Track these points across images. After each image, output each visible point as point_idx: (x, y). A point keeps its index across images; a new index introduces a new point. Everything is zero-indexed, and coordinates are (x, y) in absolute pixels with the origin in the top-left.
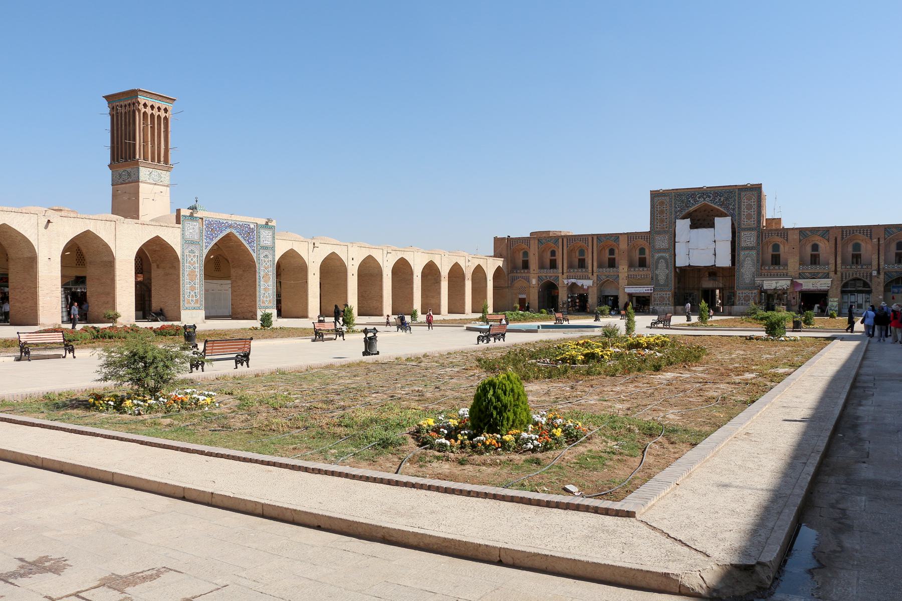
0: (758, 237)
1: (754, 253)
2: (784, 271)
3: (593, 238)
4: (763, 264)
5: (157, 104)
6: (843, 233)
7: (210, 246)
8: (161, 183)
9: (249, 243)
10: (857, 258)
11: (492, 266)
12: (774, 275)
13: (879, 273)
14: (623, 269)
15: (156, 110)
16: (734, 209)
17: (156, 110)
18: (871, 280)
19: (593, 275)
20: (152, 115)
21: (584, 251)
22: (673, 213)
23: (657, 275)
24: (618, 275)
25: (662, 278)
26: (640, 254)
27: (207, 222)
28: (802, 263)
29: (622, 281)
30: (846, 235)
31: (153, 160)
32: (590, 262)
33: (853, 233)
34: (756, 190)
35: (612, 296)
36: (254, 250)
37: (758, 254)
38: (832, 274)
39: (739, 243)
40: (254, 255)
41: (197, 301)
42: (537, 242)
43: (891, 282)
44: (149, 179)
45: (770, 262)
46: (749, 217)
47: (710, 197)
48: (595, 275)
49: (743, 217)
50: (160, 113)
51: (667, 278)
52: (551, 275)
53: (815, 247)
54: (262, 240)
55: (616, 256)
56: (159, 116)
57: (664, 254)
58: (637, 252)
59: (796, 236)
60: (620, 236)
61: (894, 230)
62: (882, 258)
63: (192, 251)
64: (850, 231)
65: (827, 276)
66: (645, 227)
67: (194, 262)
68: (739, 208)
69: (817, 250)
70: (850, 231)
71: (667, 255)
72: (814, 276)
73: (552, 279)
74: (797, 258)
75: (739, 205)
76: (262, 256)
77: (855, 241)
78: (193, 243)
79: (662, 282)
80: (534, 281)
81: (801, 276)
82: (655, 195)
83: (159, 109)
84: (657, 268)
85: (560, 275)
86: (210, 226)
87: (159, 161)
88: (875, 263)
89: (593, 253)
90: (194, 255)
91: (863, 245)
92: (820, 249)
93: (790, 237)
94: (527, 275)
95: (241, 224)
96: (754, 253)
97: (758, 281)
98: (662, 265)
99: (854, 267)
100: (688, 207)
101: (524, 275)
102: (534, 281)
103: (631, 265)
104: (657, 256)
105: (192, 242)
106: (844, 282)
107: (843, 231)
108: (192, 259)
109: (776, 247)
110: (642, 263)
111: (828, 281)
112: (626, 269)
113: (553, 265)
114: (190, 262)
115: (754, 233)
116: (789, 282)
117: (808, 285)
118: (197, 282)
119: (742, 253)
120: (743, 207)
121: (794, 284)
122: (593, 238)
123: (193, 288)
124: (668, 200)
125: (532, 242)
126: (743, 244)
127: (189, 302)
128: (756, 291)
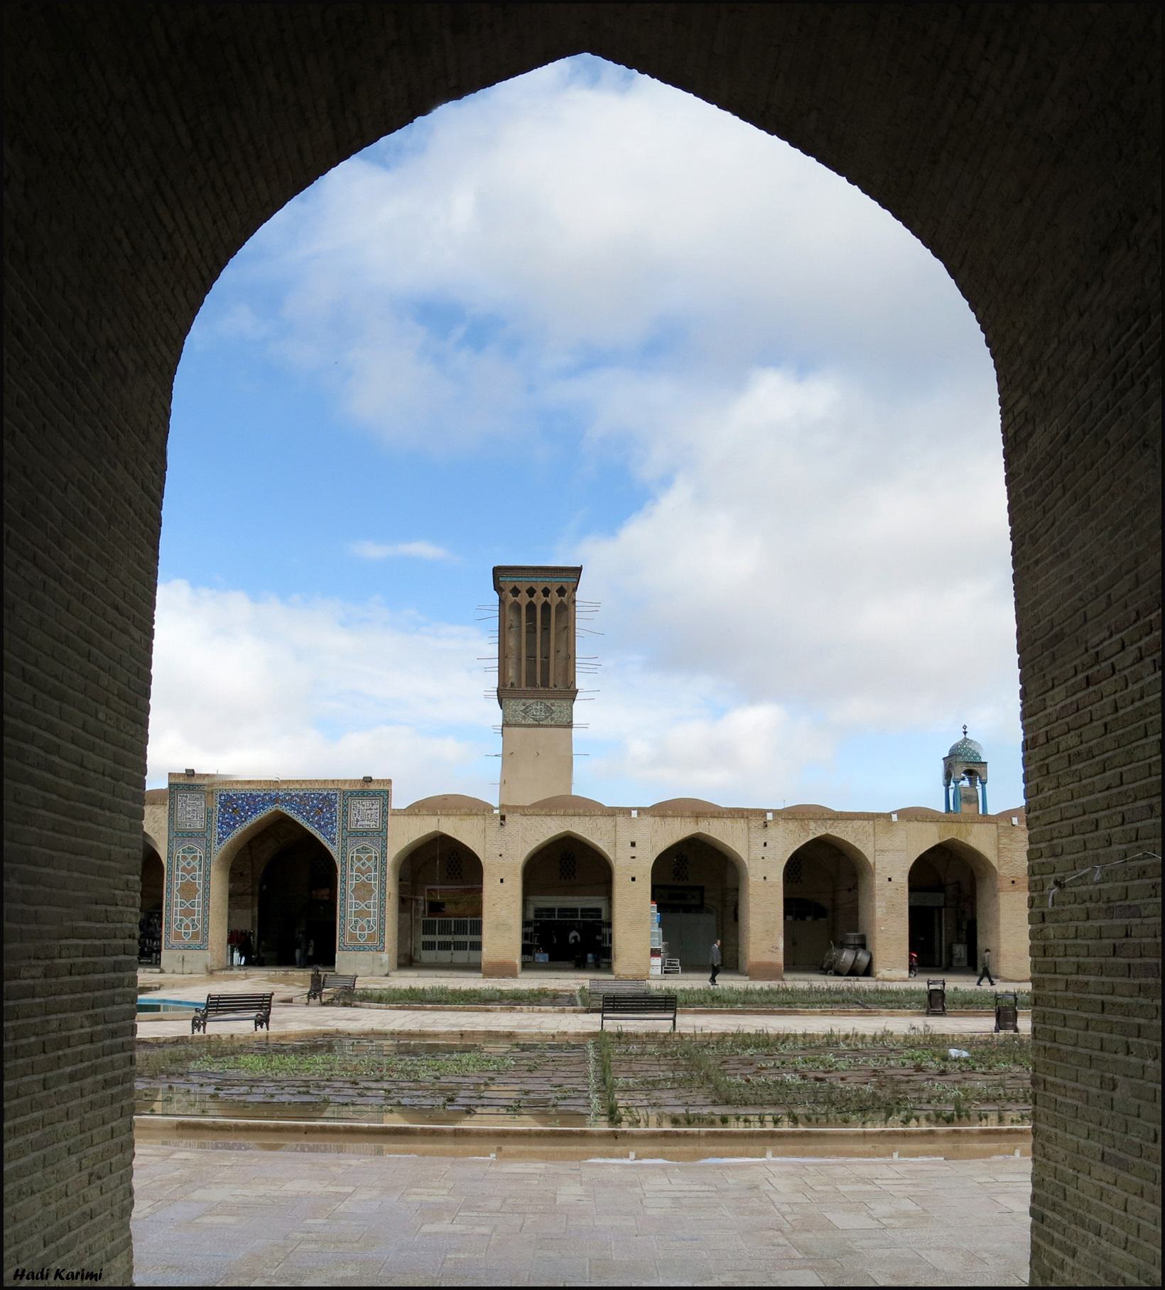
5: (540, 583)
7: (229, 840)
8: (553, 723)
9: (320, 827)
15: (539, 593)
17: (539, 593)
20: (531, 607)
27: (223, 798)
31: (531, 681)
36: (332, 840)
40: (334, 851)
41: (195, 935)
44: (524, 718)
50: (548, 599)
54: (353, 819)
56: (546, 606)
63: (191, 850)
67: (193, 867)
76: (352, 852)
78: (190, 835)
83: (546, 592)
86: (229, 804)
87: (545, 683)
90: (195, 857)
95: (301, 793)
105: (190, 835)
108: (188, 864)
114: (184, 869)
118: (176, 907)
123: (188, 913)
127: (178, 936)
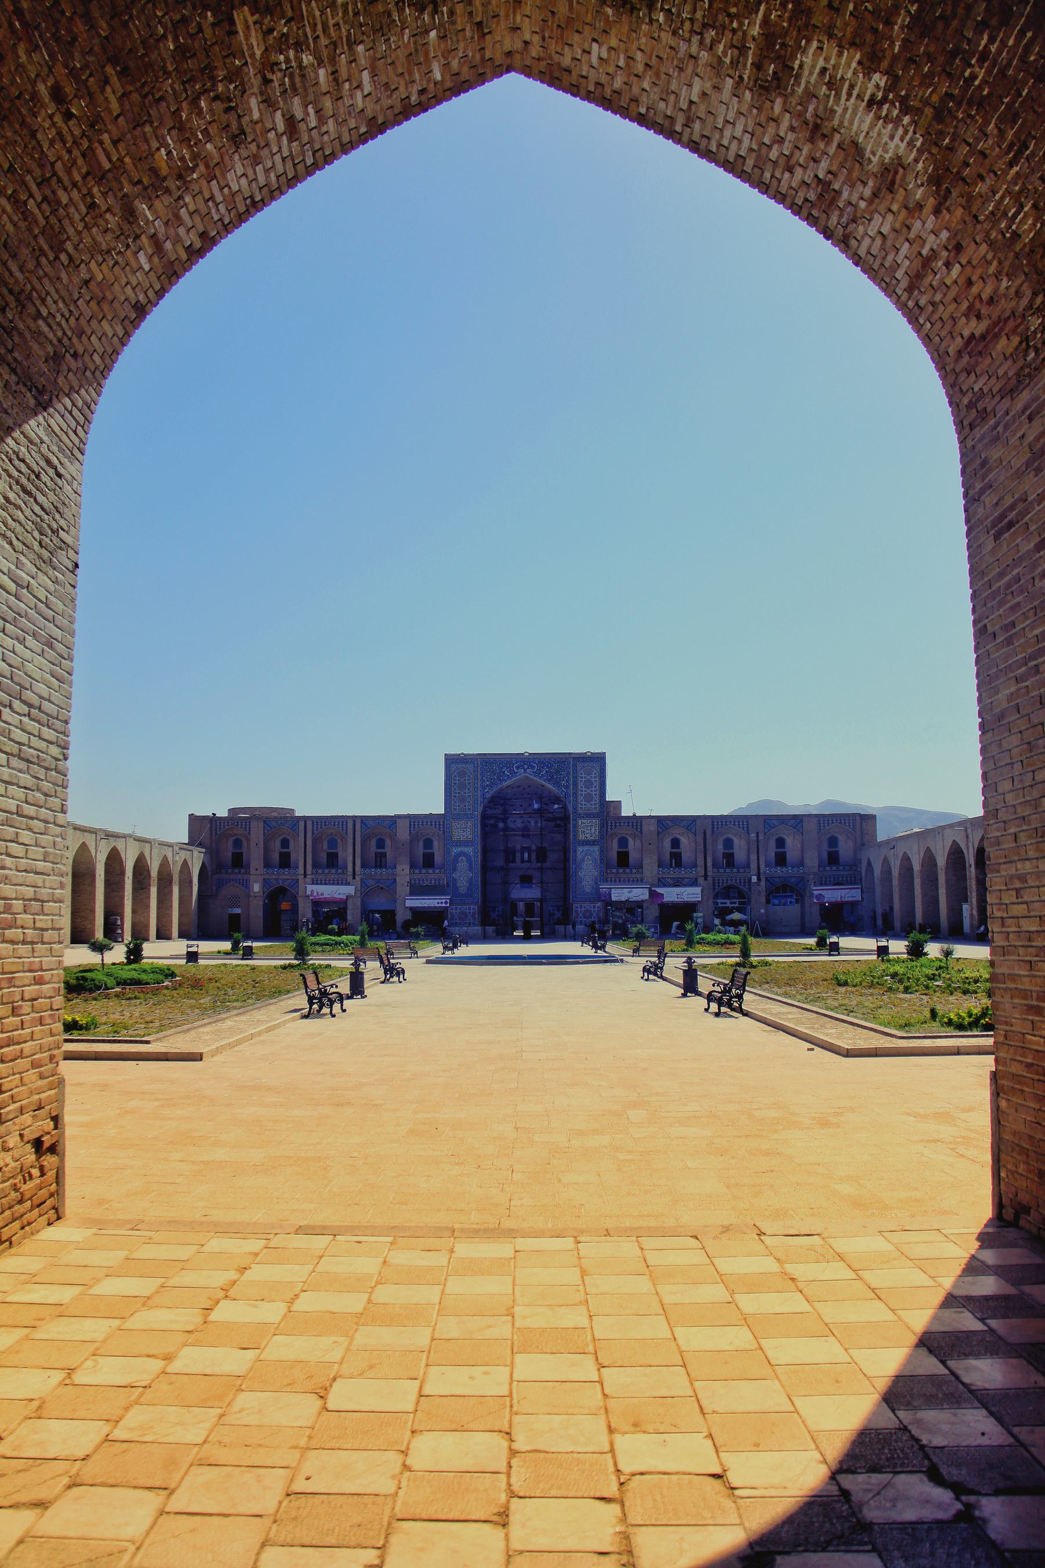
0: (601, 827)
1: (596, 849)
2: (639, 876)
3: (354, 822)
4: (608, 866)
6: (713, 825)
10: (729, 858)
11: (196, 860)
12: (624, 881)
13: (759, 879)
14: (403, 872)
16: (567, 787)
18: (750, 889)
19: (354, 878)
21: (336, 841)
22: (480, 788)
23: (455, 880)
24: (395, 880)
25: (463, 884)
26: (425, 847)
28: (661, 865)
29: (402, 887)
32: (350, 858)
34: (598, 761)
35: (379, 912)
37: (601, 851)
38: (701, 880)
39: (575, 836)
42: (261, 825)
43: (777, 890)
45: (616, 864)
46: (588, 798)
47: (533, 767)
48: (358, 878)
49: (580, 798)
51: (471, 884)
52: (285, 877)
53: (675, 843)
55: (388, 850)
57: (465, 849)
58: (421, 844)
59: (653, 828)
60: (398, 821)
61: (776, 822)
62: (762, 859)
65: (694, 883)
66: (436, 805)
68: (575, 784)
69: (678, 847)
71: (469, 850)
72: (677, 883)
73: (287, 883)
74: (656, 858)
77: (725, 836)
79: (463, 890)
80: (256, 888)
82: (451, 761)
84: (455, 870)
85: (301, 877)
88: (754, 865)
89: (354, 845)
91: (736, 841)
92: (682, 846)
93: (645, 828)
94: (245, 876)
96: (596, 849)
97: (604, 887)
98: (463, 864)
99: (728, 870)
100: (501, 781)
101: (240, 876)
102: (256, 888)
103: (413, 866)
104: (455, 850)
109: (623, 842)
110: (429, 861)
111: (698, 890)
112: (407, 870)
113: (285, 861)
115: (596, 822)
116: (647, 891)
117: (671, 895)
119: (580, 849)
120: (580, 785)
121: (653, 895)
122: (354, 822)
124: (472, 770)
125: (254, 824)
126: (581, 837)
128: (599, 904)
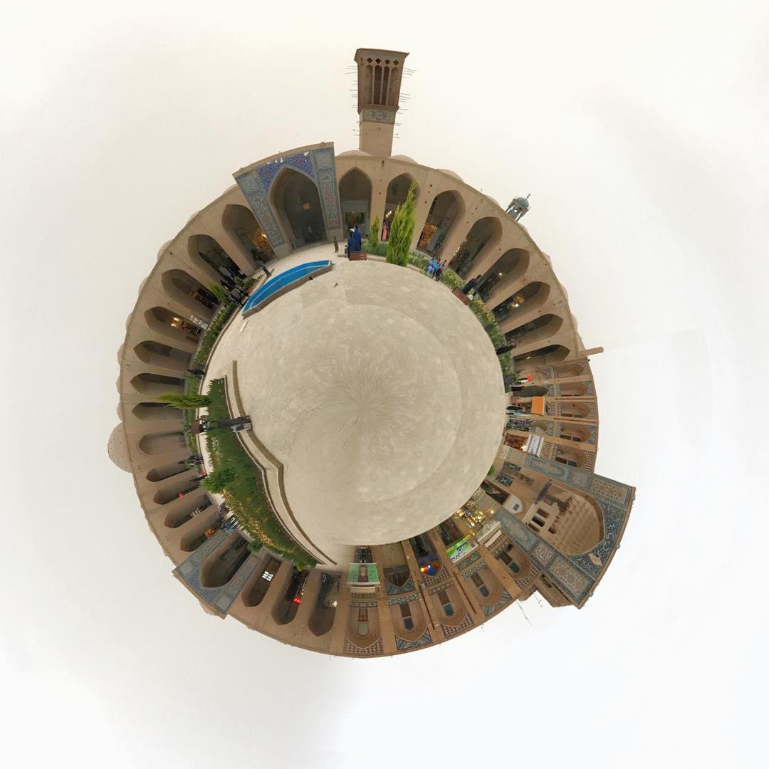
0: (539, 563)
1: (528, 547)
2: (492, 550)
6: (471, 620)
28: (486, 567)
30: (467, 620)
33: (461, 625)
38: (456, 571)
61: (422, 642)
64: (466, 626)
65: (459, 565)
70: (466, 626)
75: (580, 571)
81: (476, 554)
96: (528, 547)
106: (442, 568)
107: (473, 623)
